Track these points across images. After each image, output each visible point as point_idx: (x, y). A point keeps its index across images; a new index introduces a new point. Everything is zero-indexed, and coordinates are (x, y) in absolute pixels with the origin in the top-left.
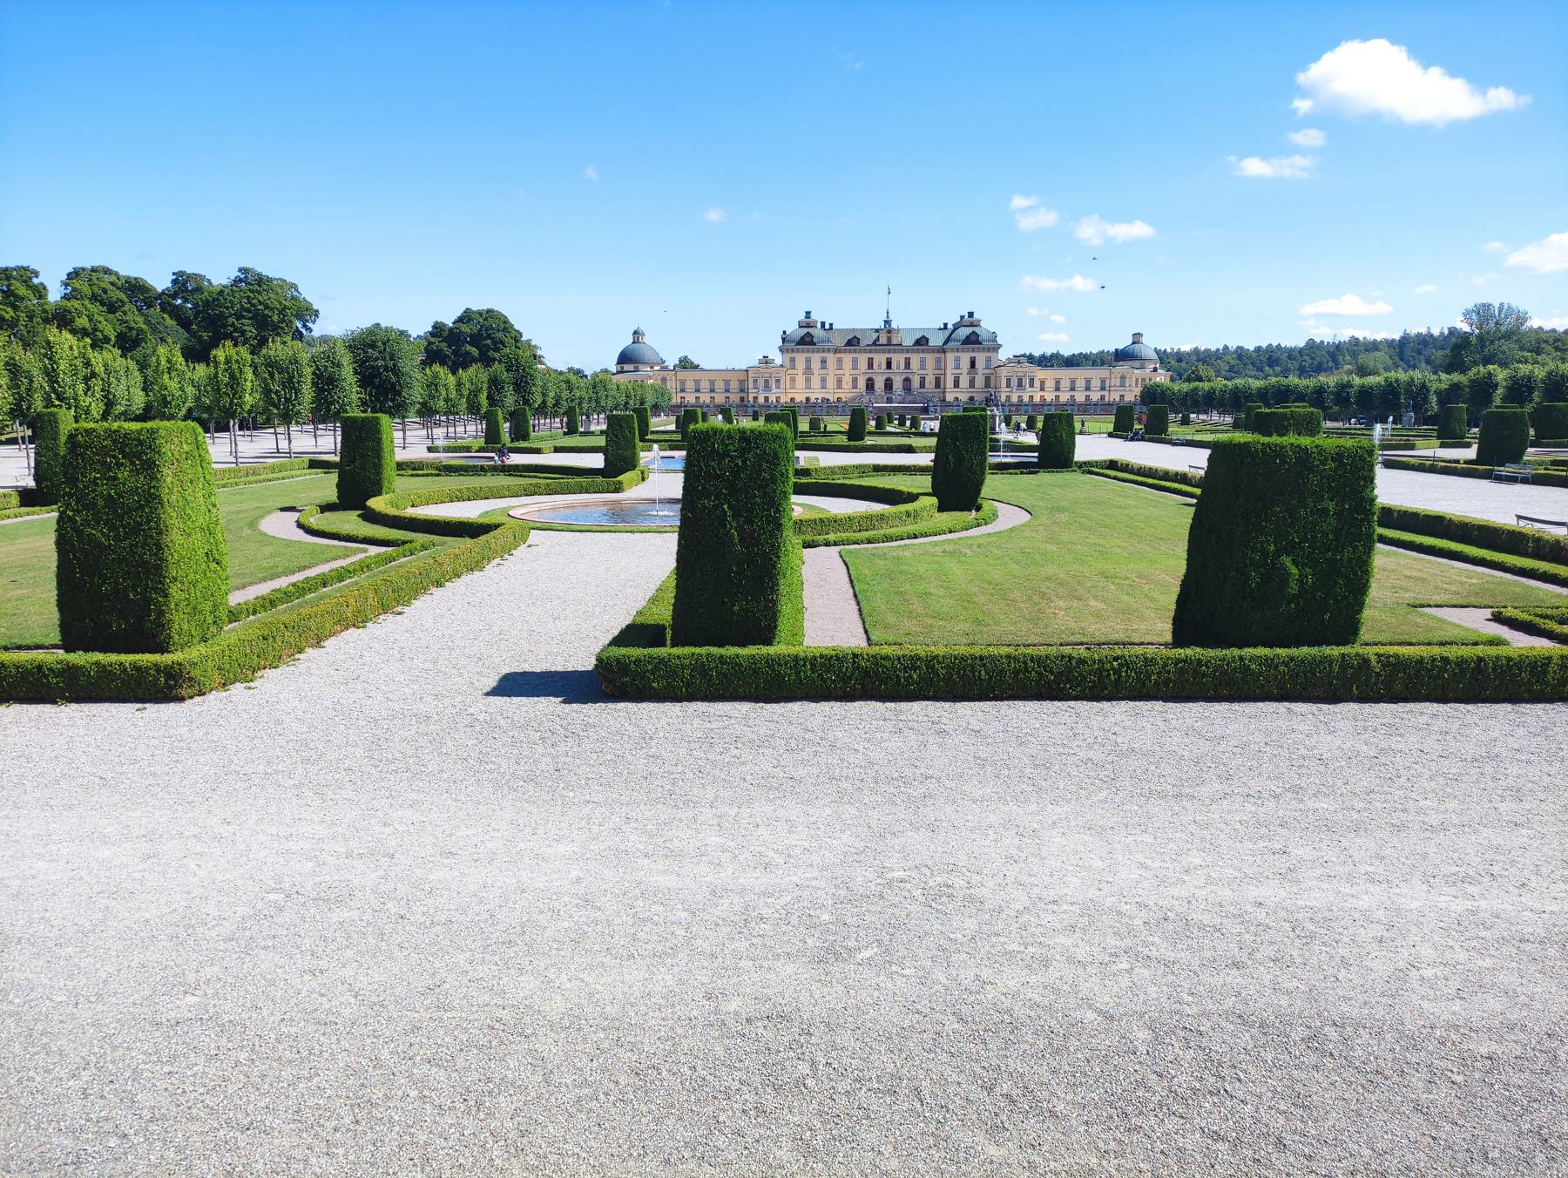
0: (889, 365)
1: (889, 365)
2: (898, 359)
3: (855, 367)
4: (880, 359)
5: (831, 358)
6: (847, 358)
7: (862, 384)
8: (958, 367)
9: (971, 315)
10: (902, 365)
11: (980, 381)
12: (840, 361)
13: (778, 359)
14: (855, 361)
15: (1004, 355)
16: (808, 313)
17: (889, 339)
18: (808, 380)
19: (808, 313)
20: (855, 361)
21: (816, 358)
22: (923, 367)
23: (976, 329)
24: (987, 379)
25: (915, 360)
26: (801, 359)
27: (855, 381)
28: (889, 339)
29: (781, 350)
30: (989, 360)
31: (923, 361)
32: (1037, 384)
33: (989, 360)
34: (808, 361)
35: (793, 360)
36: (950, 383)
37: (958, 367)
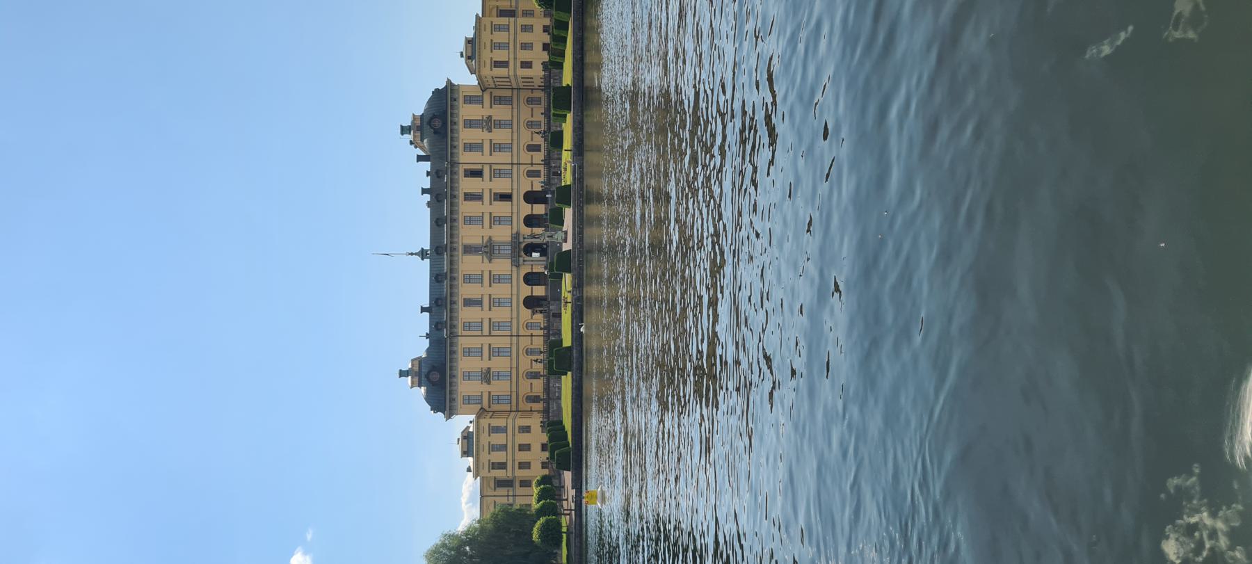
5: (463, 342)
9: (404, 130)
11: (501, 113)
12: (468, 326)
13: (463, 421)
15: (465, 79)
16: (403, 374)
18: (499, 376)
19: (403, 374)
21: (465, 364)
23: (426, 120)
24: (499, 100)
26: (465, 388)
29: (449, 417)
30: (469, 100)
32: (504, 21)
33: (469, 100)
34: (468, 376)
35: (468, 400)
36: (502, 158)
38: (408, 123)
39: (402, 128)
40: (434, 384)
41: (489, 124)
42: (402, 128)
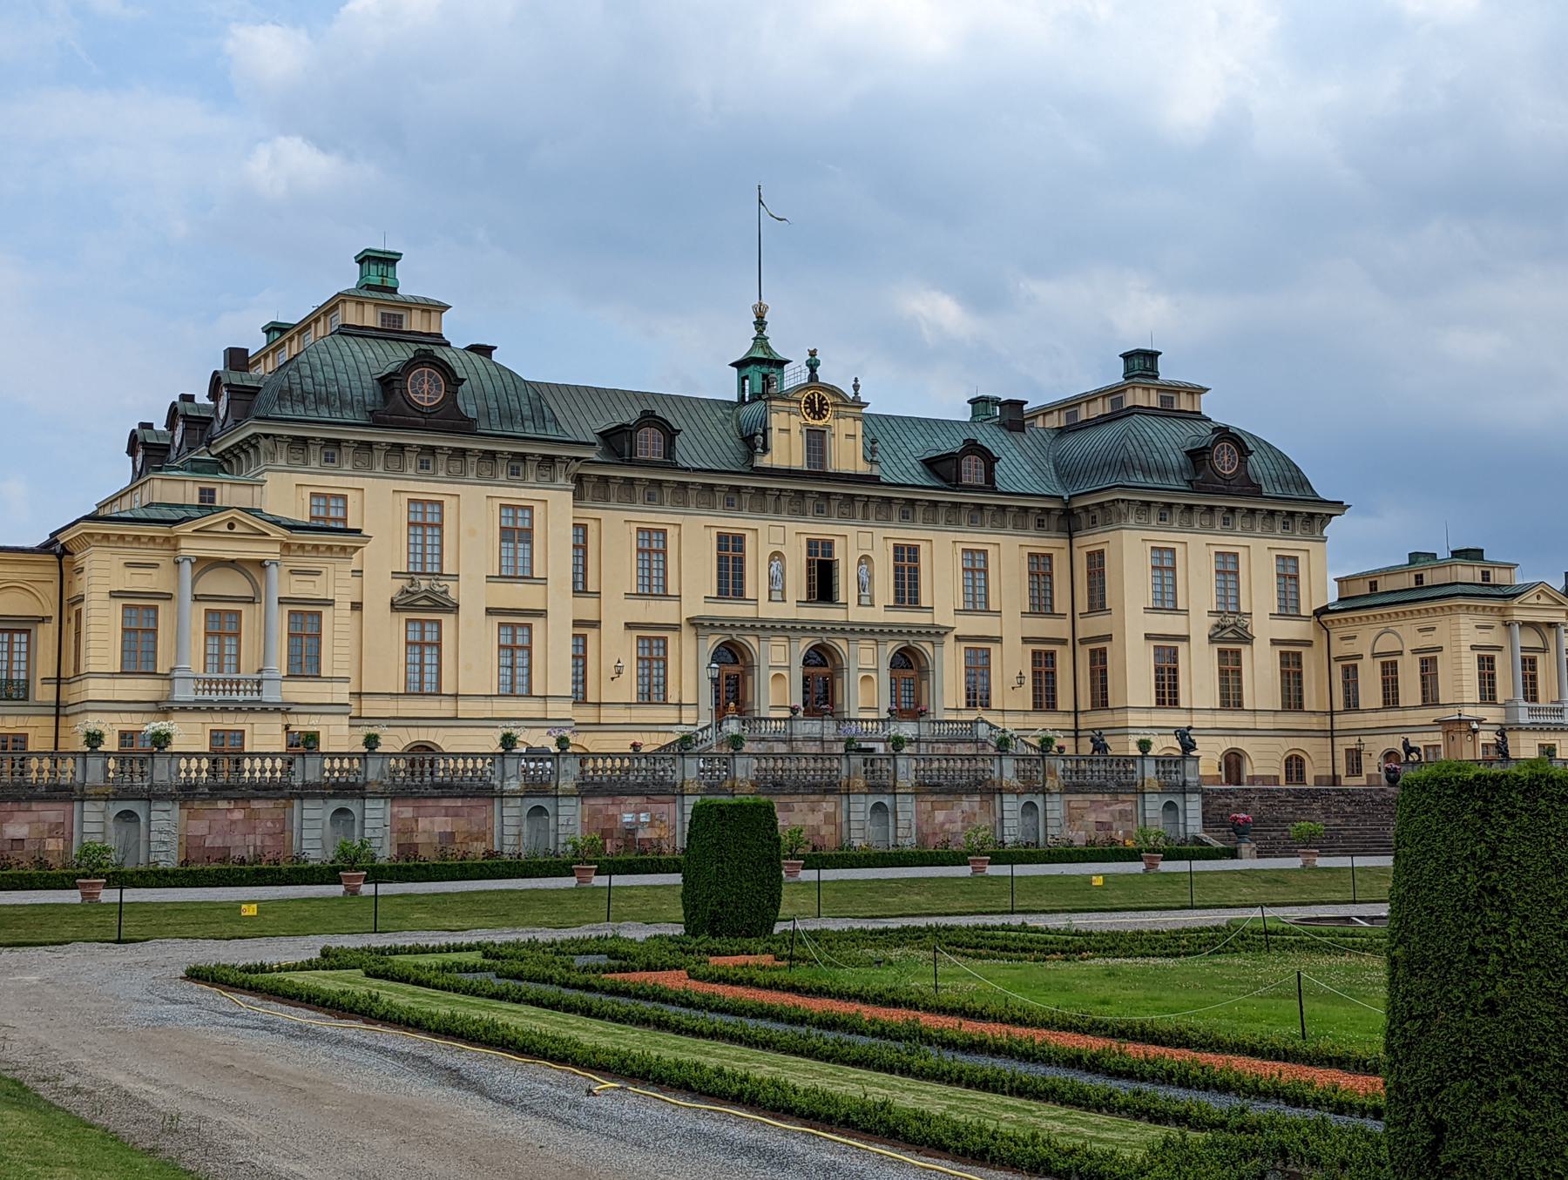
0: (823, 583)
1: (823, 583)
2: (862, 546)
3: (653, 585)
4: (776, 541)
6: (617, 527)
7: (690, 670)
8: (1166, 602)
10: (884, 587)
11: (1261, 674)
14: (652, 547)
17: (816, 441)
20: (652, 547)
22: (977, 602)
25: (942, 551)
27: (652, 644)
28: (816, 441)
30: (1288, 575)
31: (976, 566)
33: (1288, 575)
37: (1166, 602)
38: (1167, 372)
39: (1152, 356)
40: (387, 383)
41: (1231, 636)
42: (1152, 356)
